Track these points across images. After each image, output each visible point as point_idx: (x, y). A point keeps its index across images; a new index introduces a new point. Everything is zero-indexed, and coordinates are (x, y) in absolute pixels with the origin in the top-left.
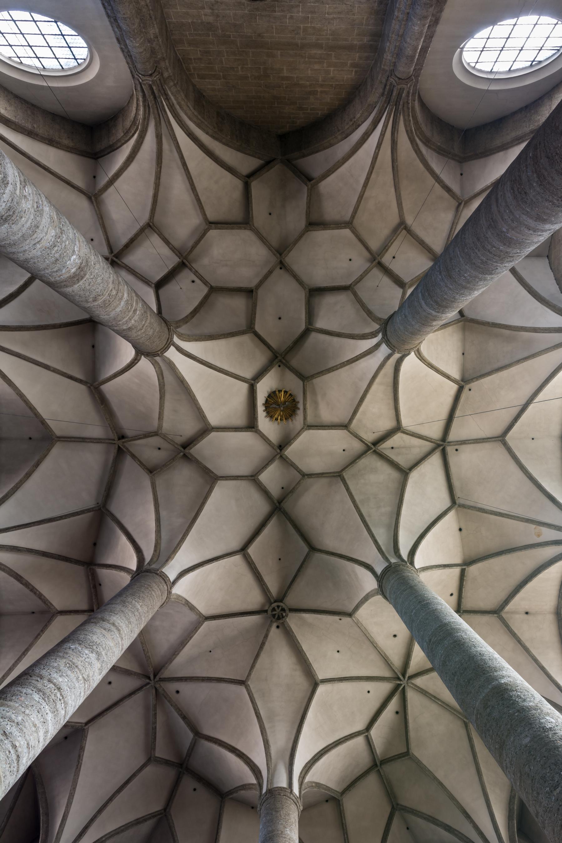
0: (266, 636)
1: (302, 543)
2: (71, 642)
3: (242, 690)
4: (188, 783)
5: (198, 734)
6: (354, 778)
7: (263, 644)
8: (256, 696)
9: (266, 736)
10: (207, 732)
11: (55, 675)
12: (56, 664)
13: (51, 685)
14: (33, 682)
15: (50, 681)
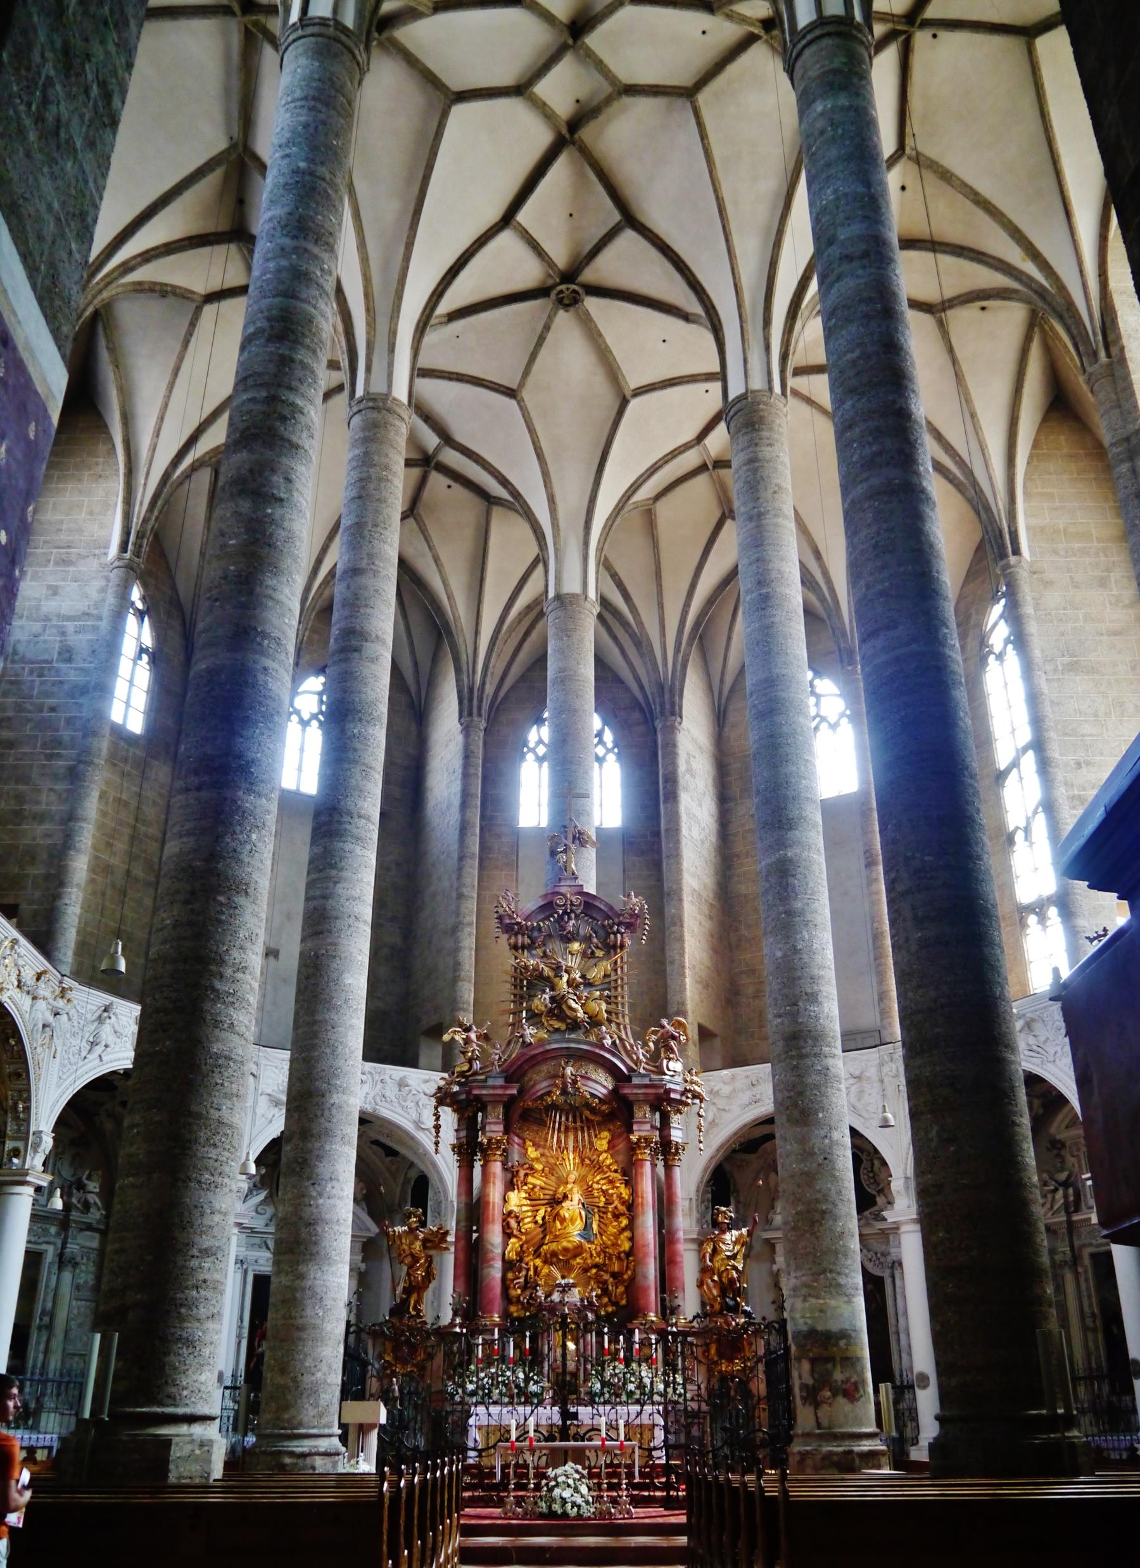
0: (547, 328)
1: (608, 203)
2: (350, 717)
3: (513, 402)
4: (437, 480)
5: (447, 439)
6: (673, 479)
7: (541, 340)
8: (534, 415)
9: (551, 488)
10: (460, 437)
11: (360, 803)
12: (353, 782)
13: (363, 821)
14: (348, 827)
15: (359, 817)
